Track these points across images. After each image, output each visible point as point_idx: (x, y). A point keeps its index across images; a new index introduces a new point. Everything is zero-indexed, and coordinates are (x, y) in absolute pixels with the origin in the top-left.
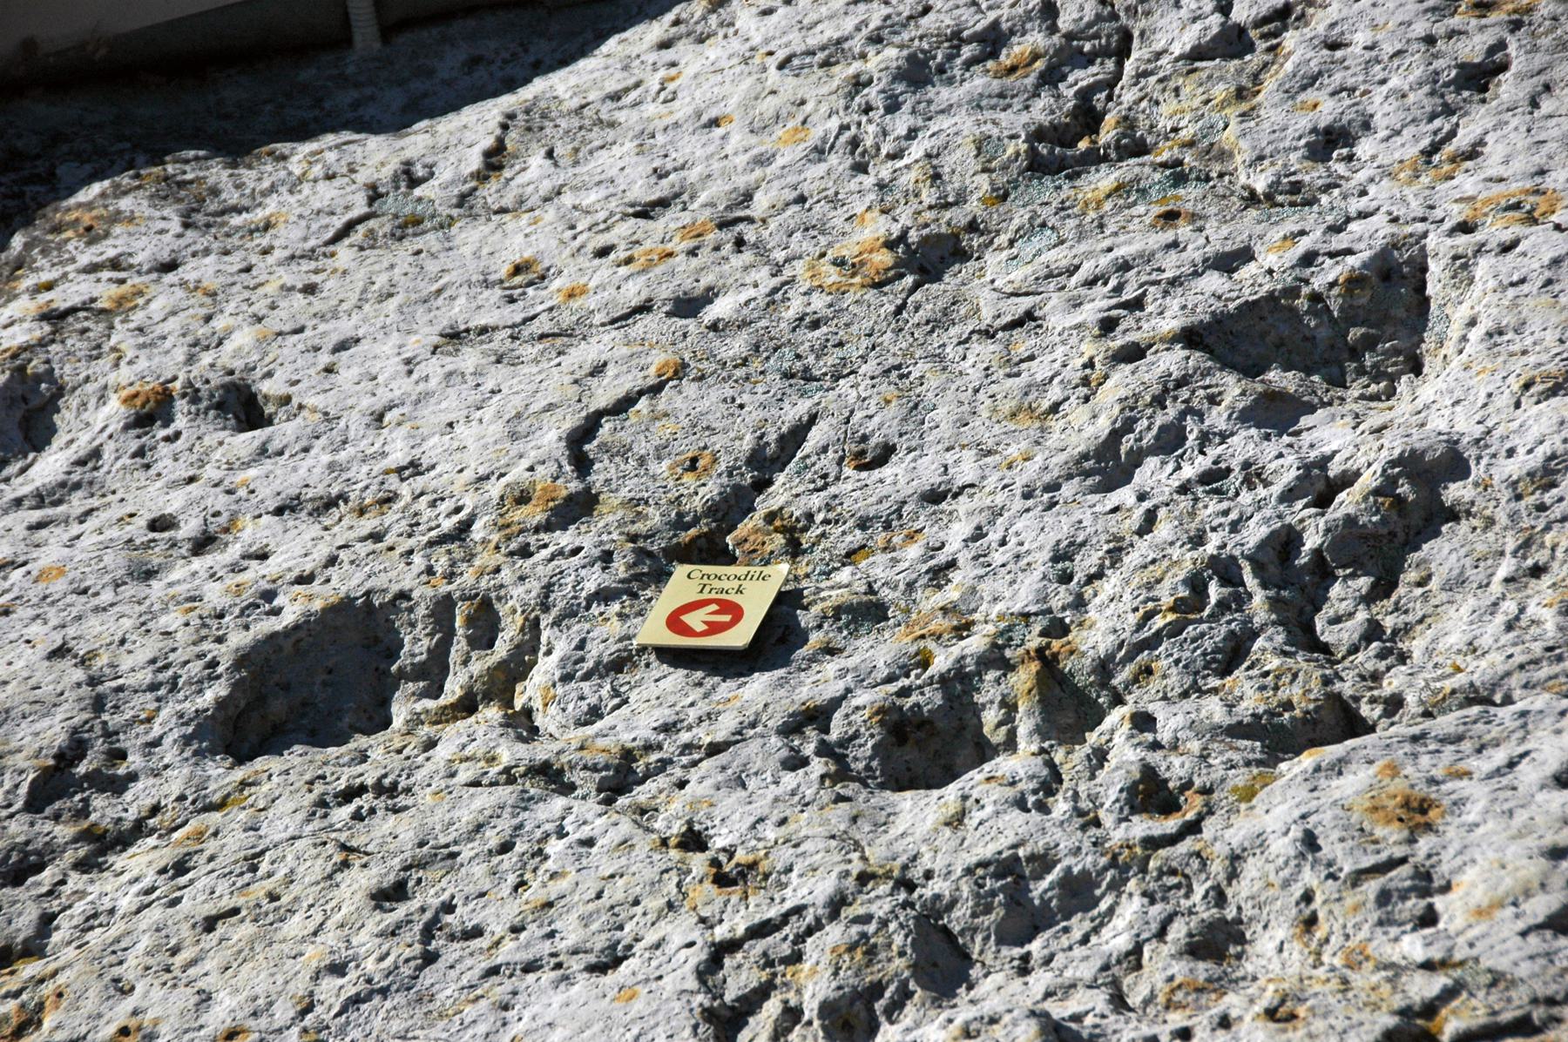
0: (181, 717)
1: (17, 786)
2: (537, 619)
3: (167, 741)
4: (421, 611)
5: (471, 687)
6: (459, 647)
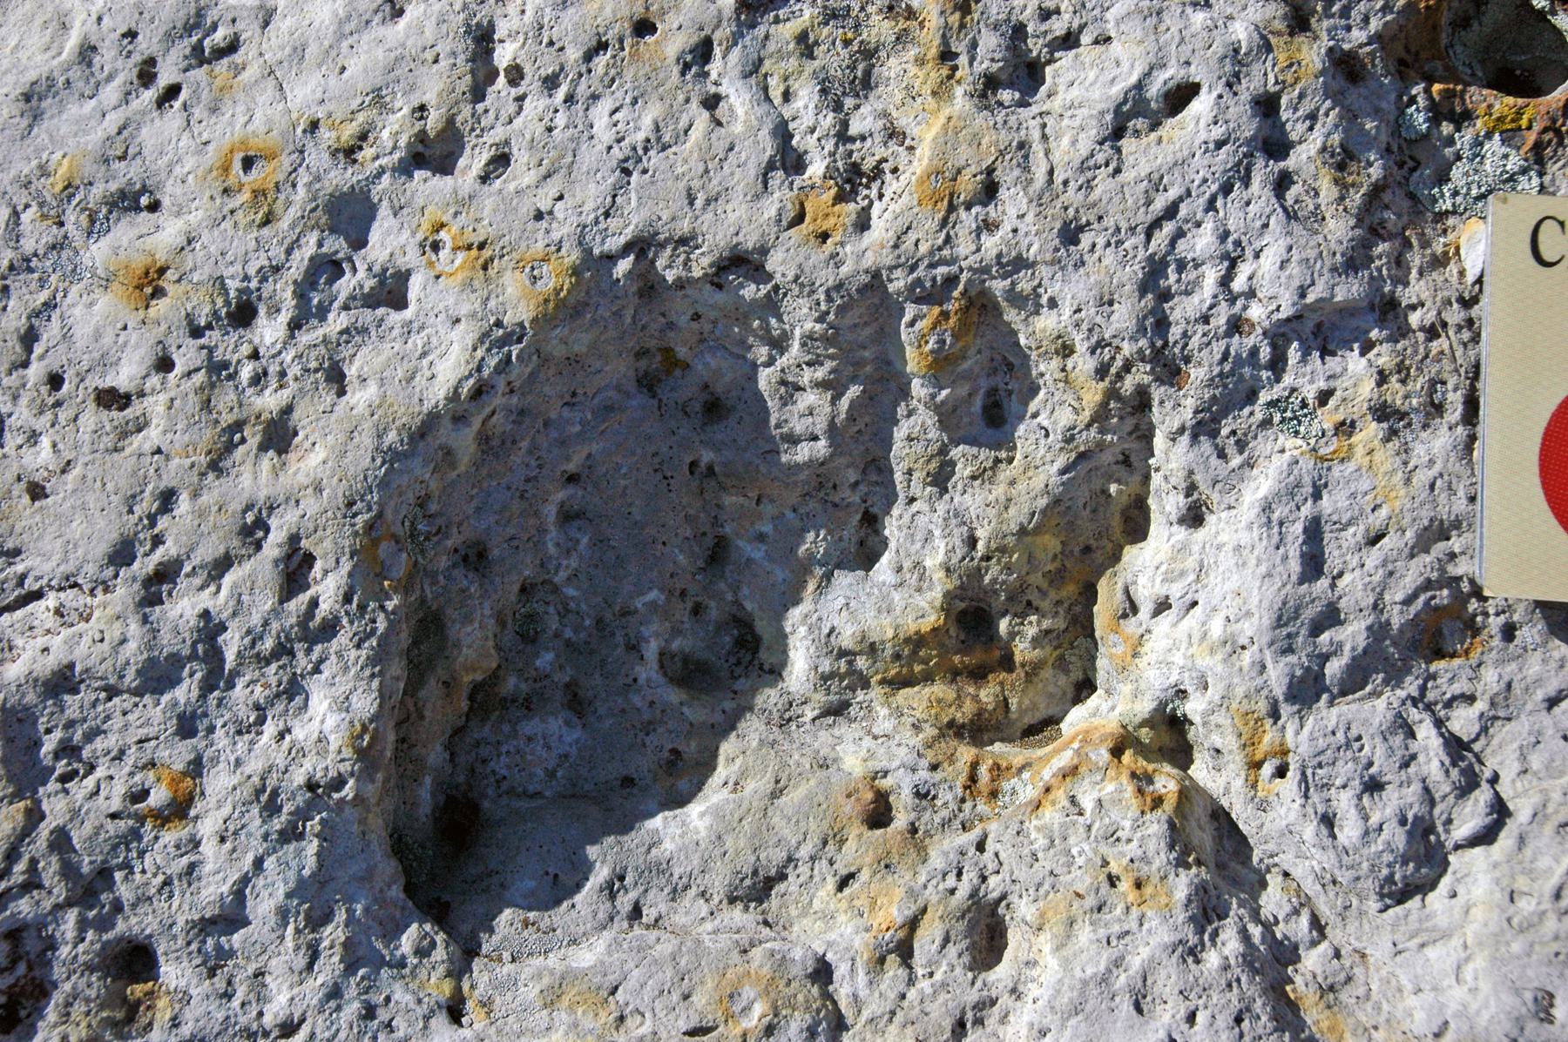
0: (272, 808)
2: (1142, 401)
3: (263, 905)
4: (801, 318)
5: (978, 573)
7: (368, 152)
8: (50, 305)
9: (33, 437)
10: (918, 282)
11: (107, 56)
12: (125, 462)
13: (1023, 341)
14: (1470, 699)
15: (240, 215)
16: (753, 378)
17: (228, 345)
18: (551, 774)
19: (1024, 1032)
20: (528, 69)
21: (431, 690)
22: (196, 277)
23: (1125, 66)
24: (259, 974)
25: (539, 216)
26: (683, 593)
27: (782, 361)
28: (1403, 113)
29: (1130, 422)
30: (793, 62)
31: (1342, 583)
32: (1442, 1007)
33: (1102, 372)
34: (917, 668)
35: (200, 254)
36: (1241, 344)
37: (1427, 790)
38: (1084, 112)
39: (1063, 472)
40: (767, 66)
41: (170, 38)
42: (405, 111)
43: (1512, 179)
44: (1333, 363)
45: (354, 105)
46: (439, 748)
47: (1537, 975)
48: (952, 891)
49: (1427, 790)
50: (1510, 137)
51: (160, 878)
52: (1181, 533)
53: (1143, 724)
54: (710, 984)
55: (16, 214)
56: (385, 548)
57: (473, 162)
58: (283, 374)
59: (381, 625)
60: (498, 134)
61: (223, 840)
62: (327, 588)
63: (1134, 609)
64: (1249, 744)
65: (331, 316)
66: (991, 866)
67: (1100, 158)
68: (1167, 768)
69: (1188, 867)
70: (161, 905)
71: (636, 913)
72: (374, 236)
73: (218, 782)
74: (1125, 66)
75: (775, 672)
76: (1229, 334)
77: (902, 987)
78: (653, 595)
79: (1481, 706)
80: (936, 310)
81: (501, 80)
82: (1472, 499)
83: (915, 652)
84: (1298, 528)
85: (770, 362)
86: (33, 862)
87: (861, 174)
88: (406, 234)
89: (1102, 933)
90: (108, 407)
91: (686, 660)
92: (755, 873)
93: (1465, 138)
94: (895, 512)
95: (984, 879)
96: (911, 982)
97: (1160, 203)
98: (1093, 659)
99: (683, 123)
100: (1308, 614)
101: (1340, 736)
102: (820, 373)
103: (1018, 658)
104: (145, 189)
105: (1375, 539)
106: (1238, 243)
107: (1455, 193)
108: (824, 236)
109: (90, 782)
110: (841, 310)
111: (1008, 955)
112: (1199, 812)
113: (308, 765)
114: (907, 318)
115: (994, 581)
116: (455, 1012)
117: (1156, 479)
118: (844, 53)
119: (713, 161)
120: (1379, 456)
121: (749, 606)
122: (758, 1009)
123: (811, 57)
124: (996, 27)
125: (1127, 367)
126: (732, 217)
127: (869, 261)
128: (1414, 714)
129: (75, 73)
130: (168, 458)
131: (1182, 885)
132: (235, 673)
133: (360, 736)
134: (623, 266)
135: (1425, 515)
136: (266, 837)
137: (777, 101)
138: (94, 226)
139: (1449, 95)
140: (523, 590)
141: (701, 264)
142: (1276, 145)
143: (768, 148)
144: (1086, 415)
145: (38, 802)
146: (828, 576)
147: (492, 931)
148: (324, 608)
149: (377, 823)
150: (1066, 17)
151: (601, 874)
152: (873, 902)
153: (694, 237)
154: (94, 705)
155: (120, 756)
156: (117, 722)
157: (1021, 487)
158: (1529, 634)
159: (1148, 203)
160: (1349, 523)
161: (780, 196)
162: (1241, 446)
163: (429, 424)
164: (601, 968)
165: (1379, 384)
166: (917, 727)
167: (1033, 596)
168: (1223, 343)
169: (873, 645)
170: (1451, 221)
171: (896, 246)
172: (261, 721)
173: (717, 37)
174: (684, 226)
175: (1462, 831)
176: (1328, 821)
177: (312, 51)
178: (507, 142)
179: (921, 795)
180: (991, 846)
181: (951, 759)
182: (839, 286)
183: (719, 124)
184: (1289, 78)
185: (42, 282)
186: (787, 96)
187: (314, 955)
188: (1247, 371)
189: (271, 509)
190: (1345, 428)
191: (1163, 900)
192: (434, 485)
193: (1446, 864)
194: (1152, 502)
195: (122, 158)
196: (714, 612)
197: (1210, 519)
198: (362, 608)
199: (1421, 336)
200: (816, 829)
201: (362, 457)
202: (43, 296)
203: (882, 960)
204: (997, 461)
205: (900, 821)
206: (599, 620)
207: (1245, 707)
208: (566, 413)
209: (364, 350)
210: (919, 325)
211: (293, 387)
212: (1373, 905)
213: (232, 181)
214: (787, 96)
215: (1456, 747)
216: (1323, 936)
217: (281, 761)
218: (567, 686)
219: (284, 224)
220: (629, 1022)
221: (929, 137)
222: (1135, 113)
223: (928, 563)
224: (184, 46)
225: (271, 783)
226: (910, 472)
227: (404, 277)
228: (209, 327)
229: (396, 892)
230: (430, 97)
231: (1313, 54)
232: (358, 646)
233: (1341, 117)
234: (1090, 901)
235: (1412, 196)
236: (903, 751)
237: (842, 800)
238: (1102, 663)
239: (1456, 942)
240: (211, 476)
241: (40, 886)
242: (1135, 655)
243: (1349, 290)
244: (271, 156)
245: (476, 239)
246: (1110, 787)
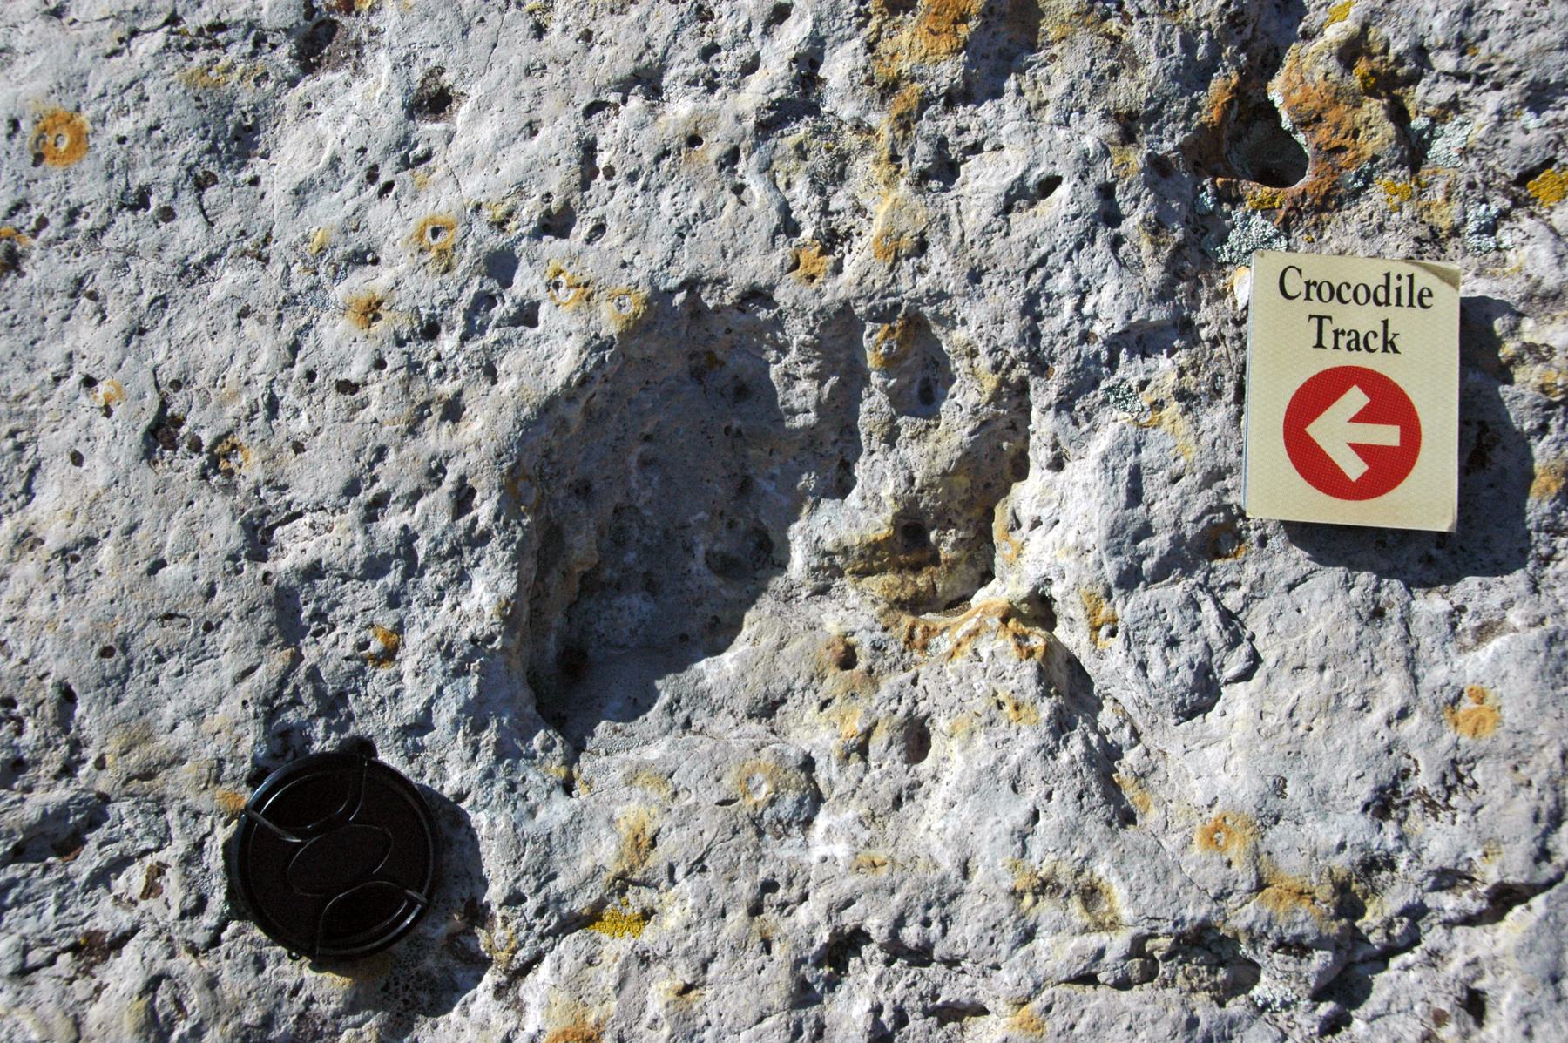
0: (448, 655)
1: (199, 846)
2: (1023, 388)
3: (443, 717)
4: (797, 332)
5: (915, 501)
6: (873, 407)
7: (513, 224)
8: (308, 326)
9: (297, 412)
10: (874, 308)
11: (347, 165)
12: (354, 428)
13: (944, 347)
14: (1238, 585)
15: (429, 266)
16: (767, 372)
17: (422, 352)
18: (633, 633)
19: (940, 804)
20: (618, 169)
21: (554, 579)
22: (401, 307)
23: (1013, 165)
24: (441, 762)
25: (624, 265)
26: (721, 514)
27: (785, 360)
28: (1197, 197)
29: (1016, 401)
30: (793, 163)
31: (1154, 509)
32: (1214, 788)
33: (996, 368)
34: (875, 564)
35: (404, 292)
36: (1088, 350)
37: (1207, 645)
38: (984, 196)
39: (971, 434)
40: (775, 165)
41: (387, 152)
42: (538, 197)
43: (1269, 241)
44: (1150, 362)
45: (504, 194)
46: (560, 615)
47: (1275, 767)
48: (895, 712)
49: (1207, 645)
50: (1268, 213)
51: (377, 699)
52: (1049, 474)
53: (1023, 601)
54: (734, 772)
55: (288, 267)
56: (521, 484)
57: (581, 230)
58: (456, 370)
59: (519, 535)
60: (598, 211)
61: (417, 675)
62: (484, 511)
63: (1019, 525)
64: (1092, 615)
65: (488, 332)
66: (921, 695)
67: (995, 226)
68: (1039, 630)
69: (1050, 696)
70: (378, 716)
71: (687, 724)
72: (517, 279)
73: (414, 637)
74: (1013, 165)
75: (782, 566)
76: (1080, 343)
77: (860, 774)
78: (701, 515)
79: (1244, 589)
80: (887, 327)
81: (601, 176)
82: (1240, 453)
83: (873, 553)
84: (1125, 472)
85: (778, 361)
86: (296, 688)
87: (837, 236)
88: (537, 277)
89: (992, 739)
90: (344, 393)
91: (724, 557)
92: (766, 698)
93: (1238, 214)
94: (861, 460)
95: (916, 703)
96: (867, 771)
97: (1035, 256)
98: (992, 557)
99: (720, 203)
100: (1131, 529)
101: (1151, 609)
102: (810, 368)
103: (942, 557)
104: (369, 250)
105: (1175, 480)
106: (1086, 283)
107: (1232, 250)
108: (812, 278)
109: (332, 636)
110: (823, 326)
111: (931, 753)
112: (1059, 659)
113: (471, 627)
114: (867, 332)
115: (926, 506)
116: (568, 787)
117: (1033, 439)
118: (827, 157)
119: (738, 229)
120: (1179, 424)
121: (765, 522)
122: (765, 788)
123: (805, 159)
124: (927, 139)
125: (1013, 365)
126: (751, 265)
127: (841, 294)
128: (1200, 595)
129: (327, 176)
130: (381, 426)
131: (1045, 708)
132: (425, 567)
133: (505, 608)
134: (680, 298)
135: (1209, 463)
136: (444, 673)
137: (782, 188)
138: (337, 275)
139: (1227, 185)
140: (616, 511)
141: (730, 297)
142: (1111, 216)
143: (775, 220)
144: (987, 396)
145: (299, 650)
146: (817, 503)
147: (593, 735)
148: (482, 524)
149: (518, 666)
150: (974, 133)
151: (664, 699)
152: (843, 718)
153: (725, 278)
154: (334, 586)
155: (352, 619)
156: (349, 598)
157: (944, 444)
158: (1276, 542)
159: (1028, 255)
160: (1160, 468)
161: (783, 251)
162: (1088, 417)
163: (553, 400)
164: (664, 760)
165: (1180, 377)
166: (875, 603)
167: (953, 516)
168: (1076, 349)
169: (846, 549)
170: (1228, 269)
171: (859, 284)
172: (441, 597)
173: (743, 146)
174: (720, 271)
175: (1231, 671)
176: (1143, 666)
177: (478, 159)
178: (604, 217)
179: (877, 648)
180: (921, 682)
181: (897, 624)
182: (822, 311)
183: (743, 203)
184: (1121, 173)
185: (304, 311)
186: (788, 185)
187: (476, 750)
188: (1092, 367)
189: (448, 459)
190: (1157, 406)
191: (1033, 718)
192: (554, 443)
193: (1220, 694)
194: (1030, 454)
195: (355, 230)
196: (742, 526)
197: (1068, 466)
198: (506, 524)
199: (1207, 345)
200: (806, 670)
201: (507, 425)
202: (304, 320)
203: (847, 757)
204: (928, 426)
205: (862, 664)
206: (666, 532)
207: (1089, 590)
208: (643, 395)
209: (509, 354)
210: (875, 337)
211: (463, 378)
212: (1171, 721)
213: (425, 244)
214: (788, 185)
215: (1227, 617)
216: (1139, 741)
217: (453, 624)
218: (645, 574)
219: (458, 272)
220: (681, 795)
221: (882, 211)
222: (1018, 197)
223: (883, 494)
224: (396, 157)
225: (447, 638)
226: (870, 434)
227: (535, 306)
228: (409, 339)
229: (530, 709)
230: (554, 187)
231: (1136, 158)
232: (504, 549)
233: (1155, 199)
234: (985, 719)
235: (1203, 252)
236: (865, 618)
237: (823, 650)
238: (997, 560)
239: (1224, 745)
240: (409, 437)
241: (301, 703)
242: (1019, 555)
243: (1159, 314)
244: (450, 228)
245: (582, 281)
246: (999, 643)
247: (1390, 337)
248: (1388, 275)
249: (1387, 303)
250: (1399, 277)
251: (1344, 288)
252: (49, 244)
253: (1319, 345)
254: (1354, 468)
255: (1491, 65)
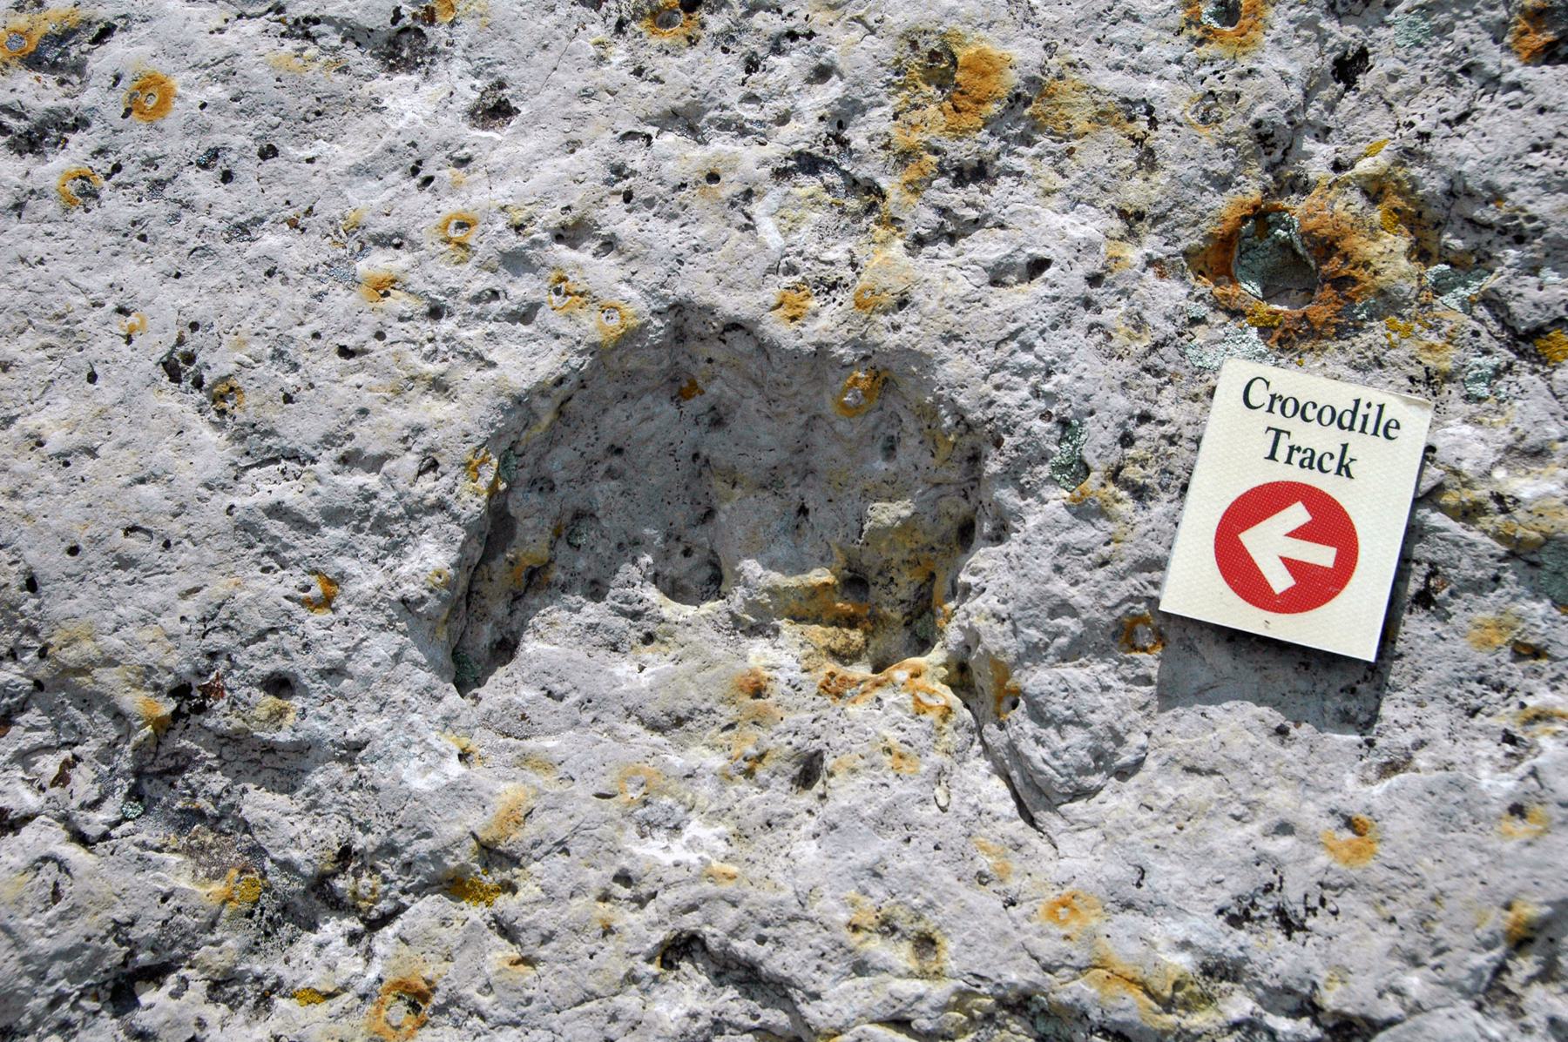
21: (498, 565)
247: (1346, 461)
248: (1357, 402)
249: (1351, 428)
250: (1369, 405)
251: (1310, 406)
252: (118, 185)
253: (1272, 457)
254: (1280, 580)
255: (1516, 218)
